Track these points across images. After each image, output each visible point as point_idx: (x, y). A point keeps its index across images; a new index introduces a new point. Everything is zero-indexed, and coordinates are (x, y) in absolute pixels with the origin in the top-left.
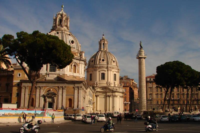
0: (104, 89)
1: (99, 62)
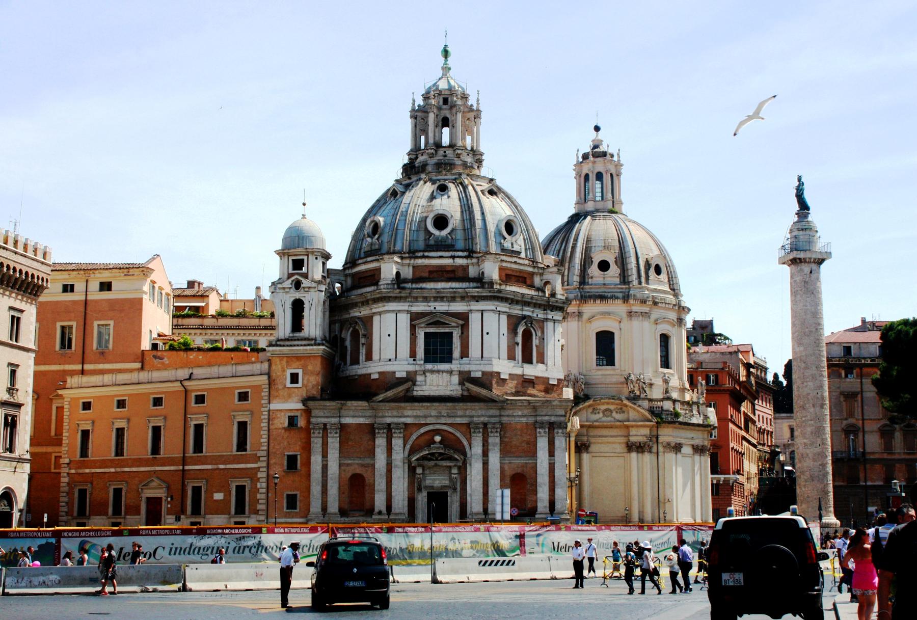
0: (614, 414)
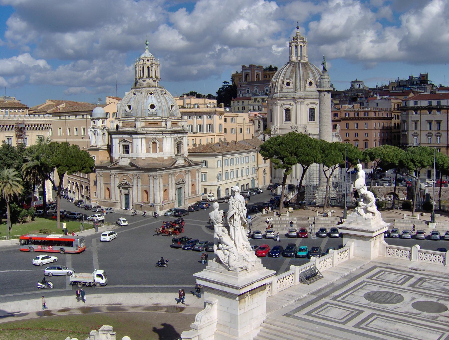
1: (282, 88)
